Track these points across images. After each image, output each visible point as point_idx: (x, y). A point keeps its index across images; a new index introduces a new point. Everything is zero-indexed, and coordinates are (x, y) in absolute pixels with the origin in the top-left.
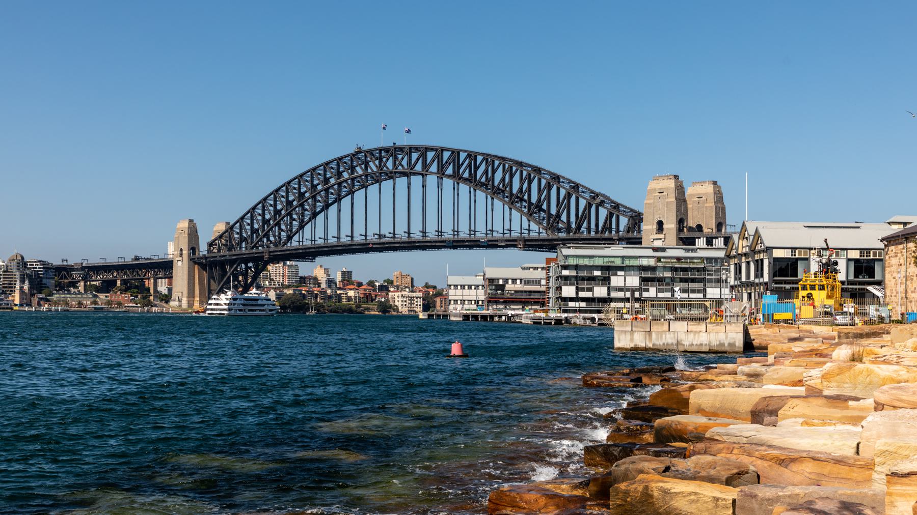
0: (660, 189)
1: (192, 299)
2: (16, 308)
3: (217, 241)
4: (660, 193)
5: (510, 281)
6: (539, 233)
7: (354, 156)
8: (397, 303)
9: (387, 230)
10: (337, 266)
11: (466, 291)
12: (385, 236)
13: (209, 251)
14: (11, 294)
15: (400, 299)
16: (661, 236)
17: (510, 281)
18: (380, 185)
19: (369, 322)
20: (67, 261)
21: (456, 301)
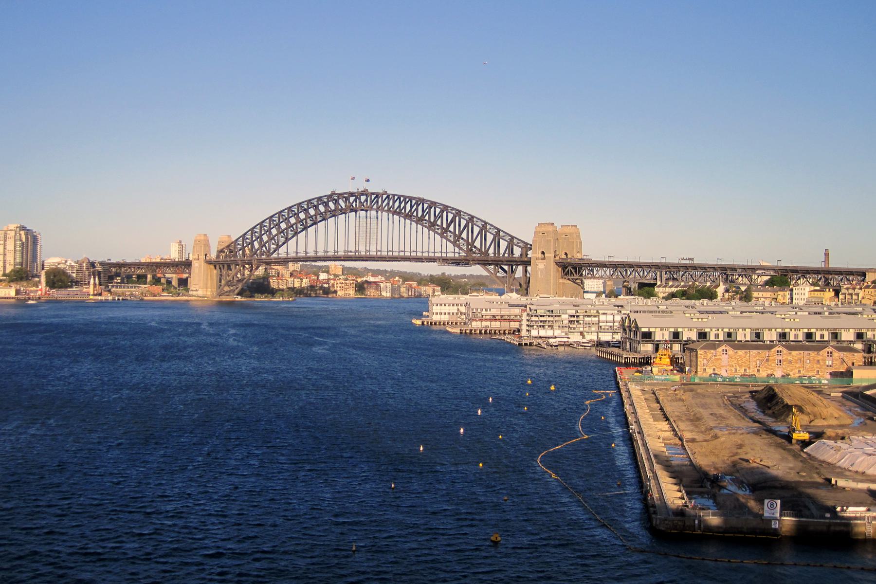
1: (205, 290)
2: (91, 297)
5: (484, 310)
6: (459, 253)
7: (330, 197)
11: (447, 307)
12: (351, 252)
13: (218, 257)
14: (615, 408)
17: (484, 310)
19: (493, 361)
21: (437, 314)
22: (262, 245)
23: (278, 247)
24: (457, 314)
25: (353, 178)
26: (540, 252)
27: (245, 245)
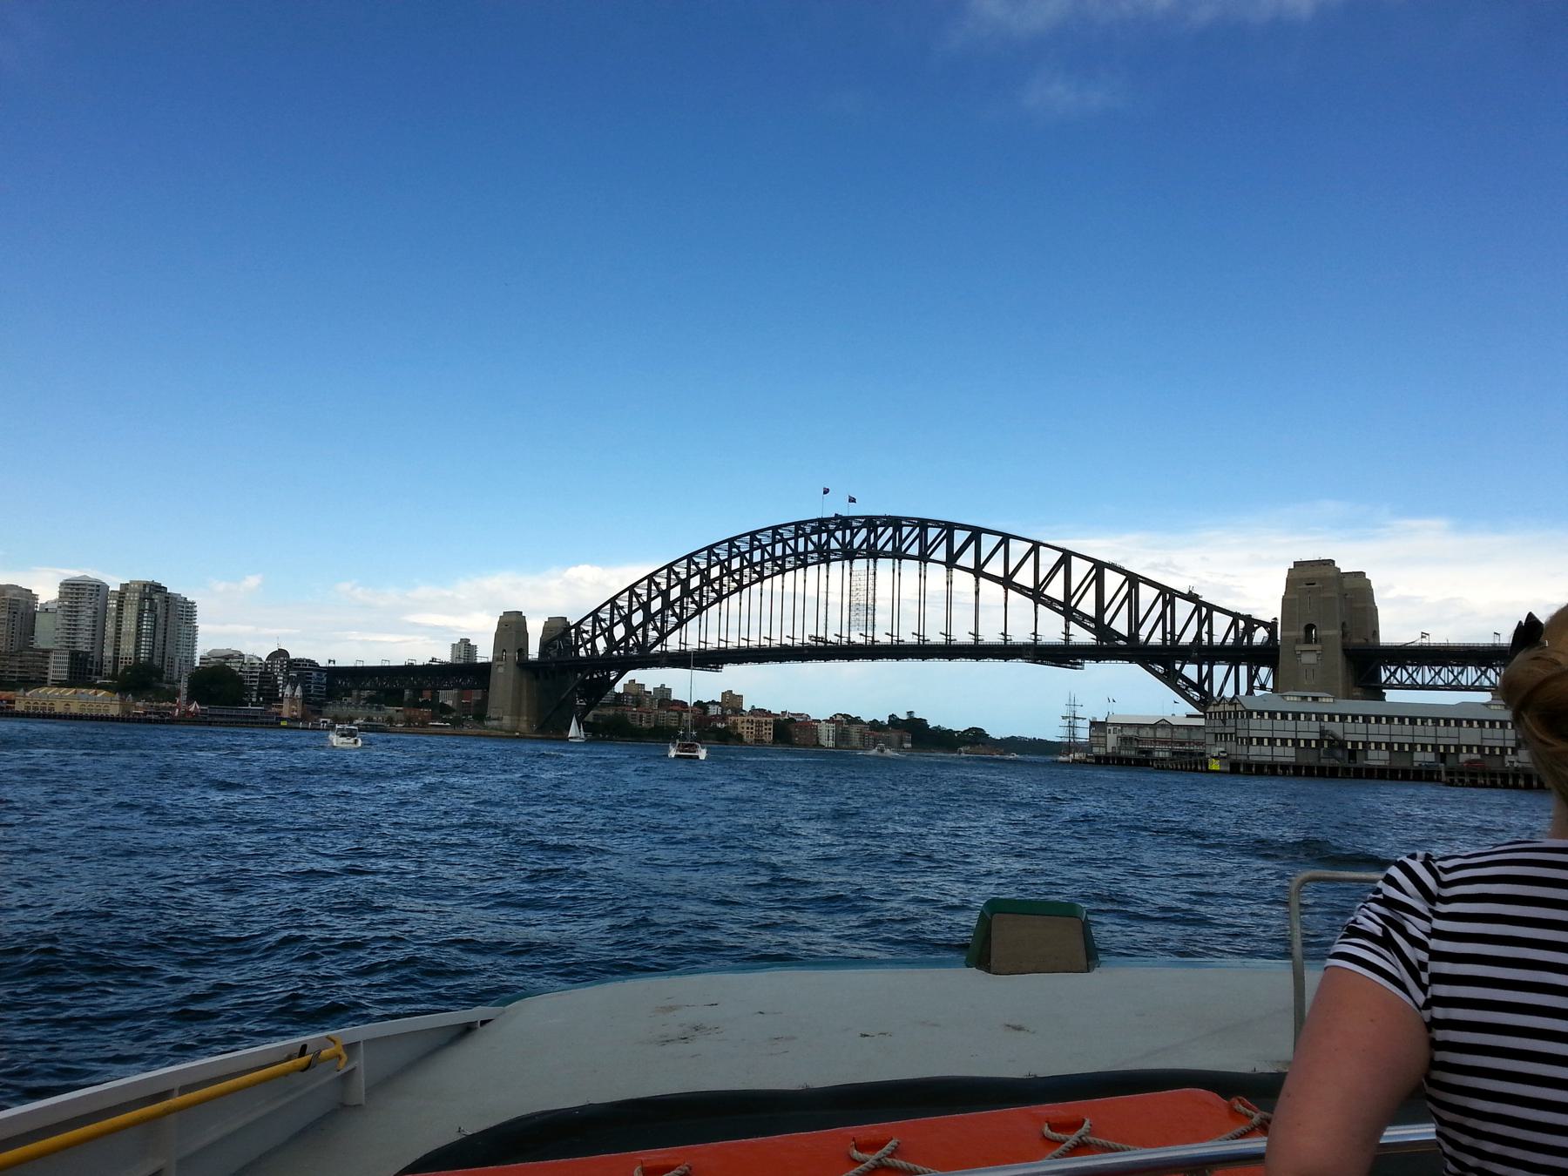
0: (1309, 579)
1: (517, 718)
3: (557, 641)
4: (1308, 584)
8: (740, 730)
9: (821, 634)
10: (733, 678)
15: (745, 725)
16: (1318, 647)
18: (805, 570)
20: (334, 662)
21: (1260, 741)
22: (630, 631)
23: (663, 636)
24: (1319, 743)
25: (826, 491)
26: (1303, 625)
27: (580, 643)
